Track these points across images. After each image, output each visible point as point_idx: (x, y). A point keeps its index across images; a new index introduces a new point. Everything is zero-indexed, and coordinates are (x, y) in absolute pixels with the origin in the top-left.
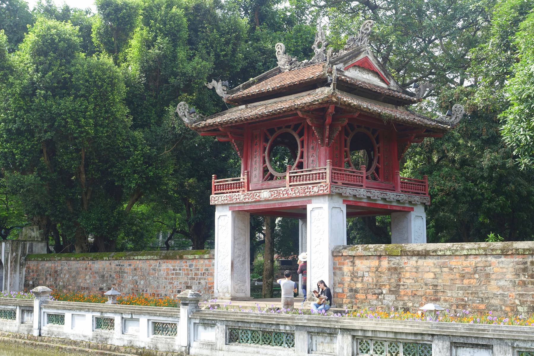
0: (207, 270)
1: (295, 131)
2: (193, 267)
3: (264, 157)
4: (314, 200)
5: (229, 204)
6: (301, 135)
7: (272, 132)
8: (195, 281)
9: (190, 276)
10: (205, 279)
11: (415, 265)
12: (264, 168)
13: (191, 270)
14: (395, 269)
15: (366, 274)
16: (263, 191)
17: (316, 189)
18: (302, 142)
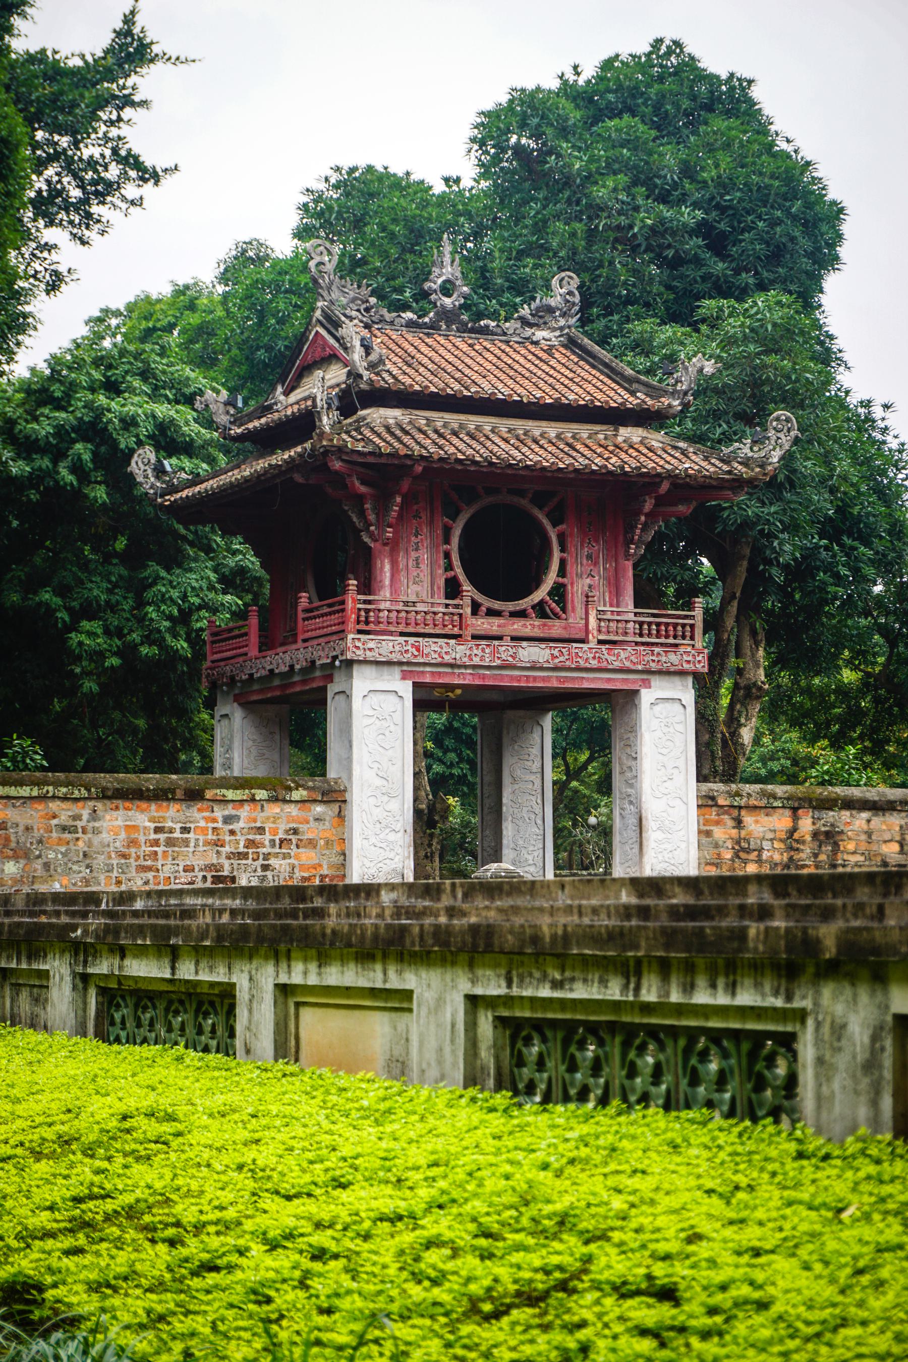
0: (295, 831)
1: (541, 508)
2: (241, 824)
3: (447, 555)
4: (656, 681)
5: (400, 663)
8: (250, 861)
9: (227, 849)
10: (286, 856)
11: (865, 827)
12: (447, 581)
13: (232, 832)
14: (827, 834)
15: (766, 845)
16: (524, 644)
17: (673, 658)
18: (562, 538)
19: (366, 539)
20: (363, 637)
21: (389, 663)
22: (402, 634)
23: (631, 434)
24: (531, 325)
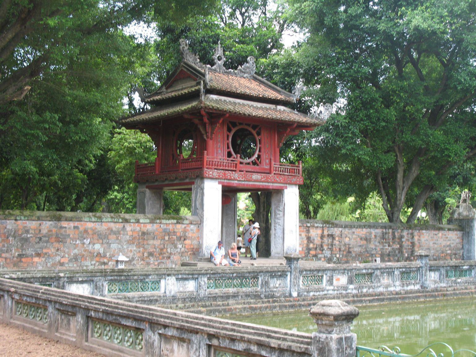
6: (259, 134)
7: (234, 125)
12: (228, 152)
16: (254, 174)
19: (205, 138)
20: (209, 170)
21: (216, 179)
22: (223, 170)
23: (281, 108)
24: (243, 72)
